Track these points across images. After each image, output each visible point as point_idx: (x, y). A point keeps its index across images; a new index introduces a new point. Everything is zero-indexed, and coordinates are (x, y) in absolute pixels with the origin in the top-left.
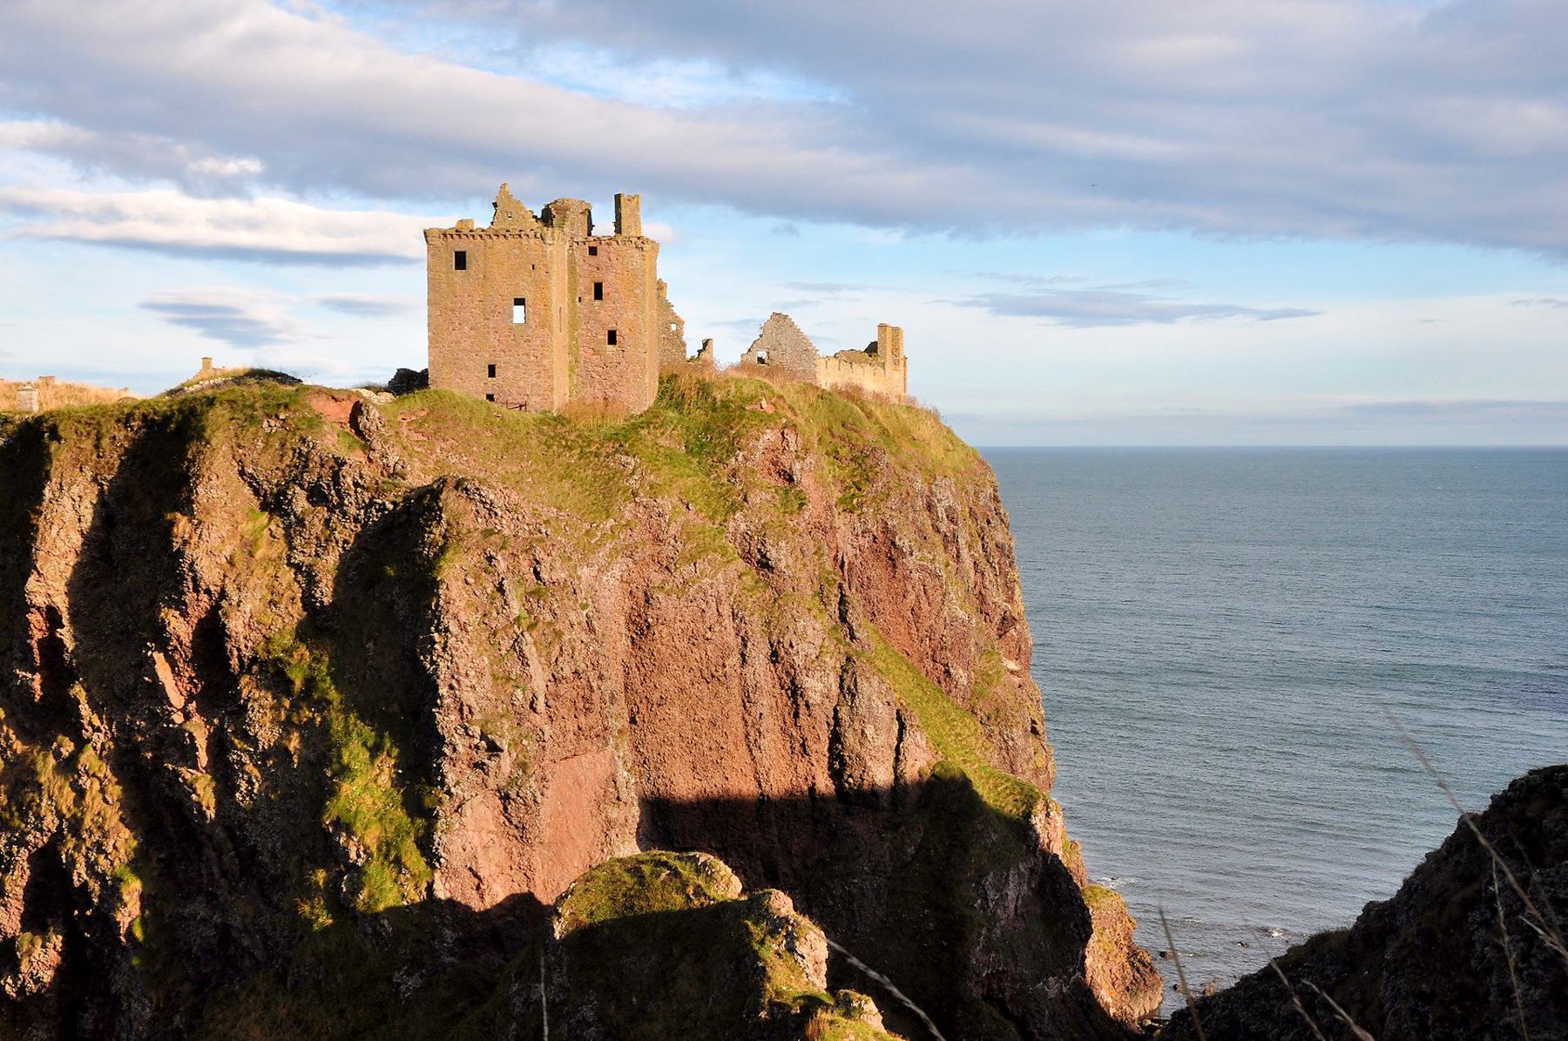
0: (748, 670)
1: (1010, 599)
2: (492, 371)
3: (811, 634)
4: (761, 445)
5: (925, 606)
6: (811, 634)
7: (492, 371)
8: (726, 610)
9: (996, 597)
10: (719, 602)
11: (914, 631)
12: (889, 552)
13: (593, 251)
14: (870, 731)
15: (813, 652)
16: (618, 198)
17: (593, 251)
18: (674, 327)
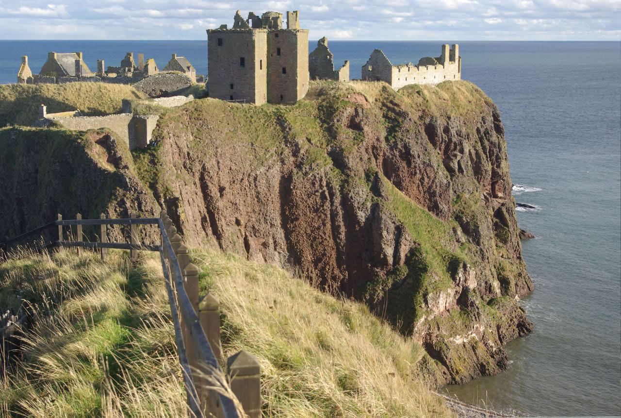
0: (334, 208)
1: (499, 166)
2: (232, 86)
3: (361, 193)
4: (345, 115)
5: (426, 180)
6: (361, 193)
7: (232, 86)
8: (324, 184)
9: (488, 167)
10: (321, 180)
11: (421, 187)
12: (407, 155)
13: (277, 35)
14: (385, 233)
15: (362, 201)
16: (288, 12)
17: (277, 35)
18: (328, 57)
